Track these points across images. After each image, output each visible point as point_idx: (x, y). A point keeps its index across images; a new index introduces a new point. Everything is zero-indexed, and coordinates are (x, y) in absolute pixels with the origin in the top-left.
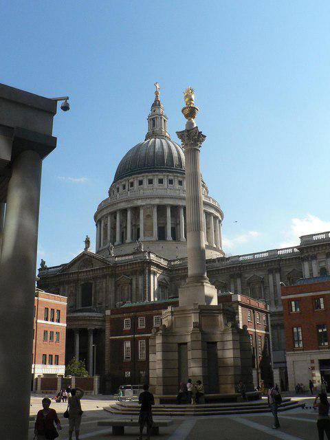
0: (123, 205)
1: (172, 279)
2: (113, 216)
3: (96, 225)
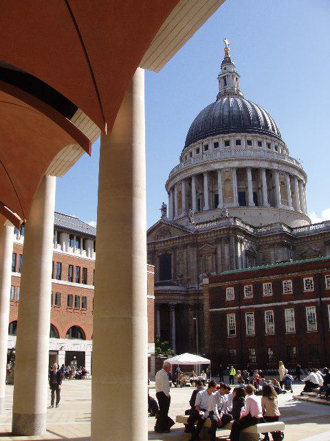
0: (198, 170)
1: (259, 248)
3: (169, 194)
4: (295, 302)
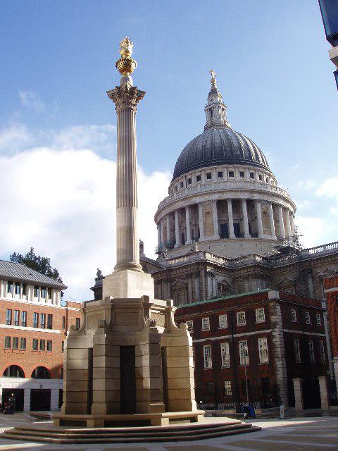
1: (234, 280)
2: (172, 217)
4: (212, 339)
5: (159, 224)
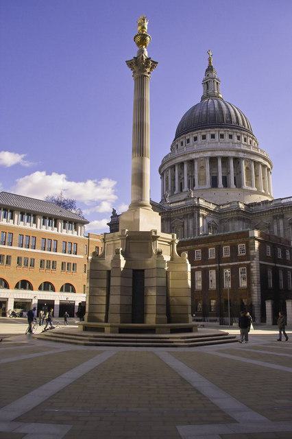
1: (221, 222)
4: (203, 267)
5: (162, 175)
